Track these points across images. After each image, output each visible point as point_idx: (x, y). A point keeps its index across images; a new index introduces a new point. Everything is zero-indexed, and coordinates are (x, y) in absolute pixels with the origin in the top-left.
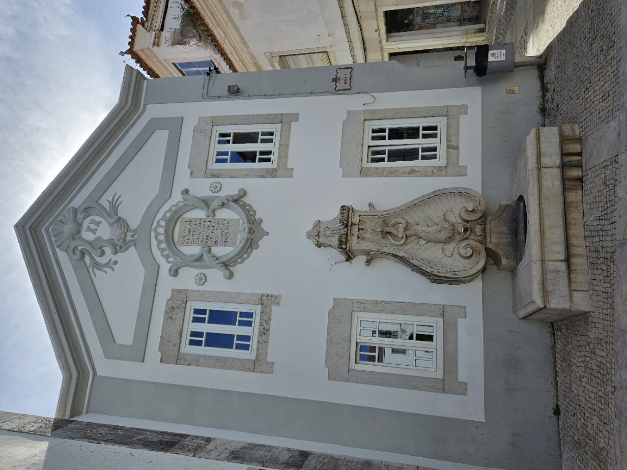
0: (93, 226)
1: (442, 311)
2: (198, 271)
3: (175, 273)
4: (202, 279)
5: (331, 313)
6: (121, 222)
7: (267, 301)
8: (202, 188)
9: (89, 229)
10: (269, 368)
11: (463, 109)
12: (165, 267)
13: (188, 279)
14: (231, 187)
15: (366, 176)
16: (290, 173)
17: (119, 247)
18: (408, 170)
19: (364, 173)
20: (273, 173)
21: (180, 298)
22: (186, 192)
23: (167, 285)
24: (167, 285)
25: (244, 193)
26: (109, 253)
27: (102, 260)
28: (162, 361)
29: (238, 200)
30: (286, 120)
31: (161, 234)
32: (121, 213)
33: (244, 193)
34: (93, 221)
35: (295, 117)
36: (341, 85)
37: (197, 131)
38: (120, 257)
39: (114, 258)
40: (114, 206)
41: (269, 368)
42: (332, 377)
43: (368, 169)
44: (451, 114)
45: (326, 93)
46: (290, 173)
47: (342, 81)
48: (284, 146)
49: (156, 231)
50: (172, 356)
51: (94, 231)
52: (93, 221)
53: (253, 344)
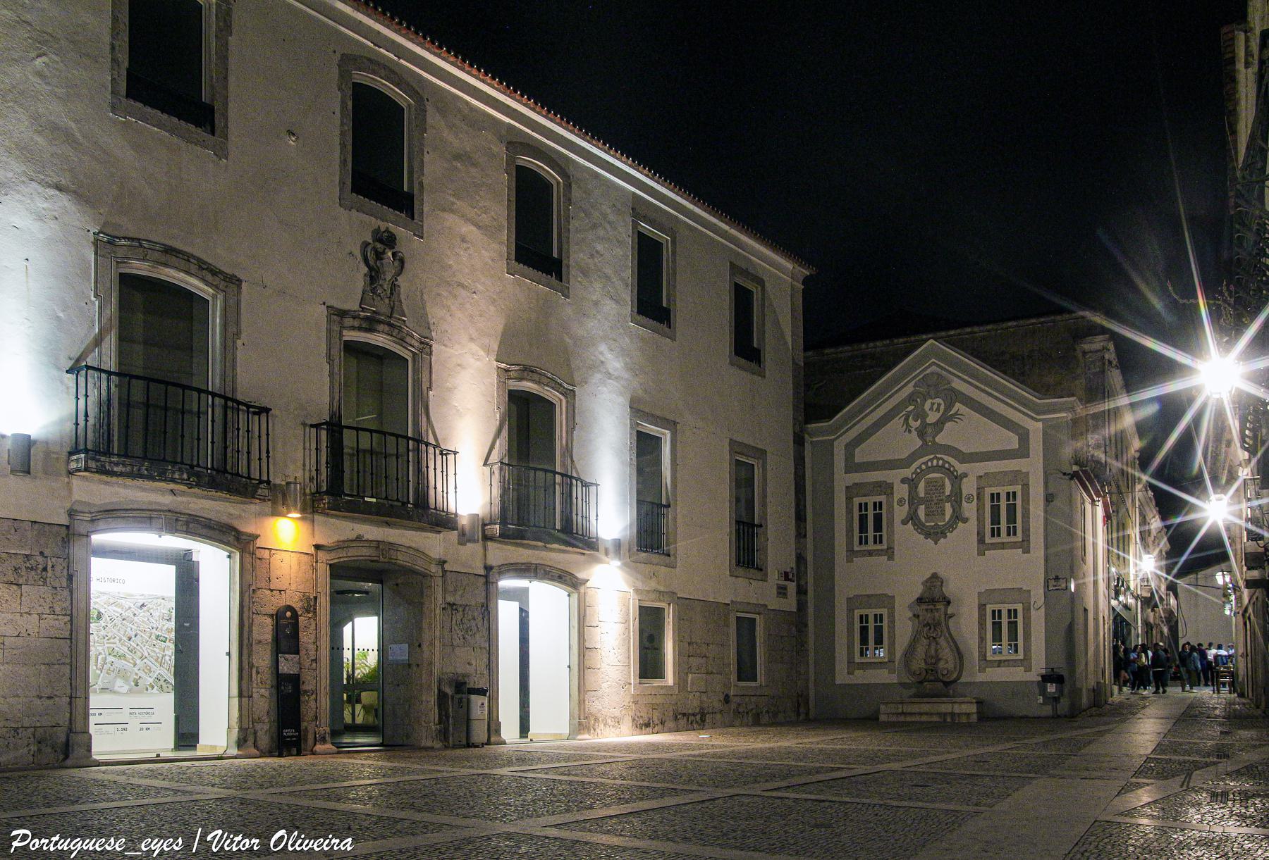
0: (935, 407)
1: (891, 661)
2: (907, 498)
3: (903, 481)
4: (901, 502)
5: (885, 595)
6: (939, 425)
7: (889, 552)
8: (969, 487)
9: (933, 404)
10: (849, 560)
11: (1028, 669)
12: (908, 473)
13: (901, 491)
14: (969, 509)
15: (979, 608)
16: (981, 553)
17: (921, 433)
18: (983, 635)
19: (982, 607)
20: (981, 540)
21: (886, 488)
22: (965, 475)
23: (894, 476)
24: (894, 476)
25: (965, 520)
26: (915, 424)
27: (911, 421)
28: (847, 487)
29: (958, 517)
30: (1025, 546)
31: (932, 463)
32: (949, 425)
33: (965, 520)
34: (939, 405)
35: (1027, 551)
36: (1052, 583)
37: (1017, 473)
38: (915, 434)
39: (913, 430)
40: (951, 418)
41: (849, 560)
42: (849, 599)
43: (985, 610)
44: (1026, 663)
45: (1046, 572)
46: (981, 553)
47: (1055, 584)
48: (1003, 546)
49: (935, 458)
50: (851, 491)
51: (931, 409)
52: (939, 405)
53: (864, 548)
